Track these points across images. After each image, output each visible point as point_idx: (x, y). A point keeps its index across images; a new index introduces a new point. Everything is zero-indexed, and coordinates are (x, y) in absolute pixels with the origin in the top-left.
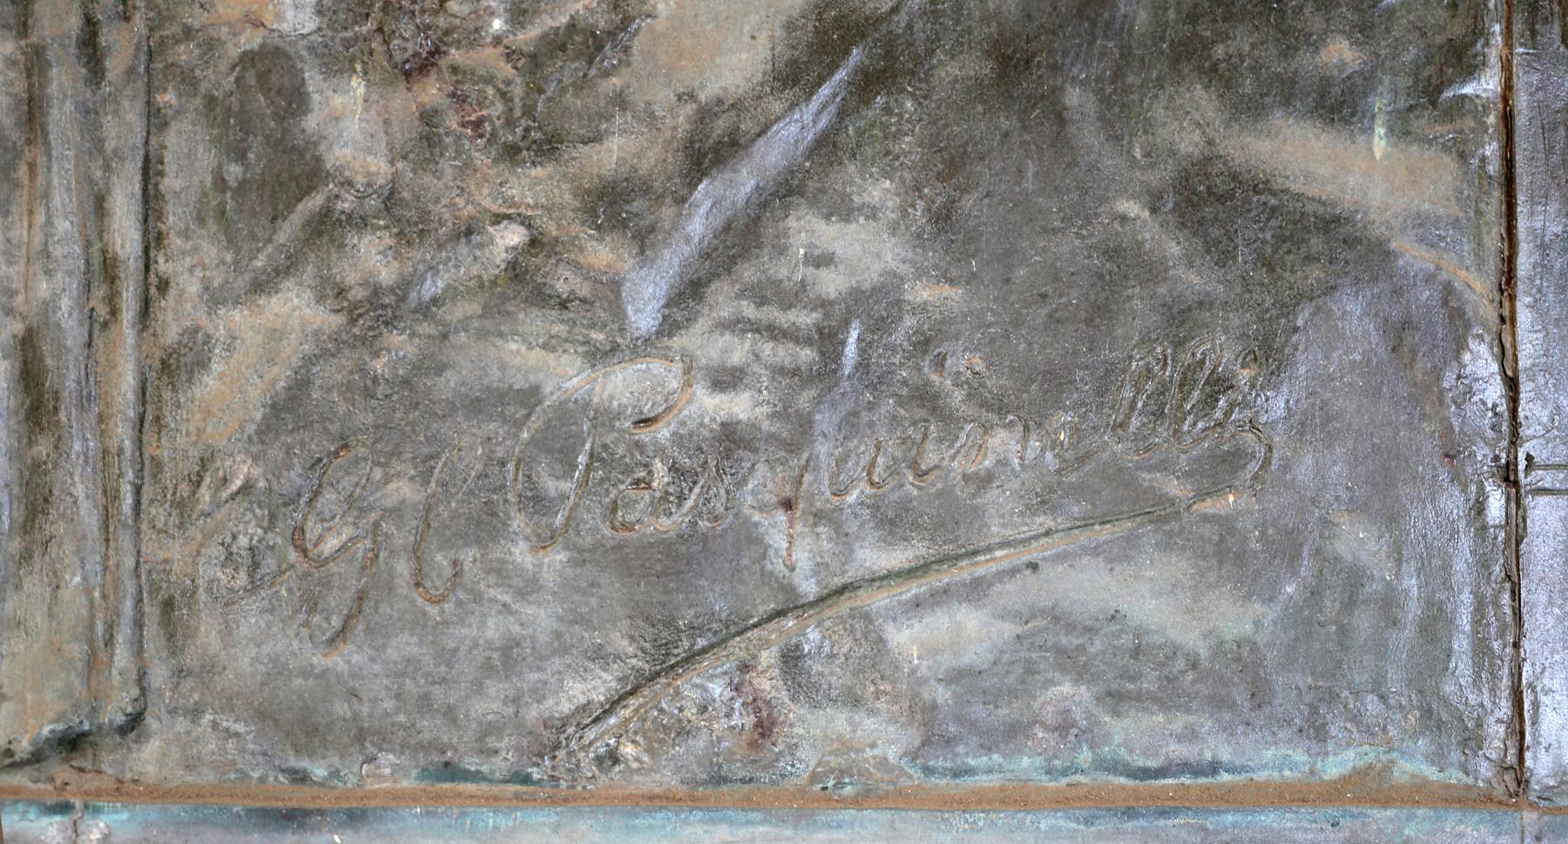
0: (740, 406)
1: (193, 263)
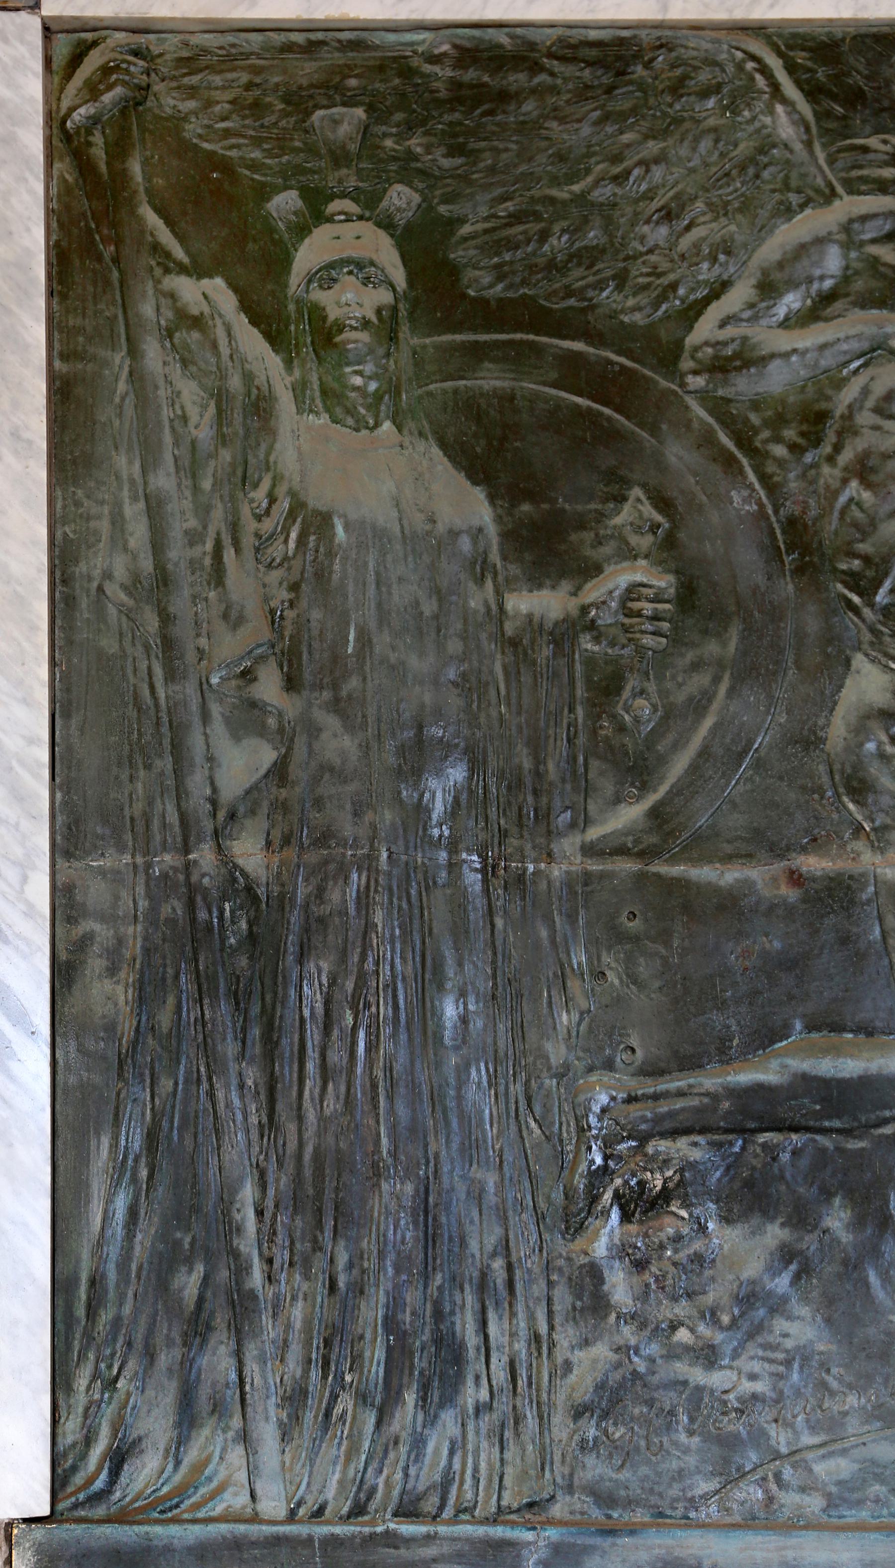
0: (759, 1387)
1: (565, 1337)
